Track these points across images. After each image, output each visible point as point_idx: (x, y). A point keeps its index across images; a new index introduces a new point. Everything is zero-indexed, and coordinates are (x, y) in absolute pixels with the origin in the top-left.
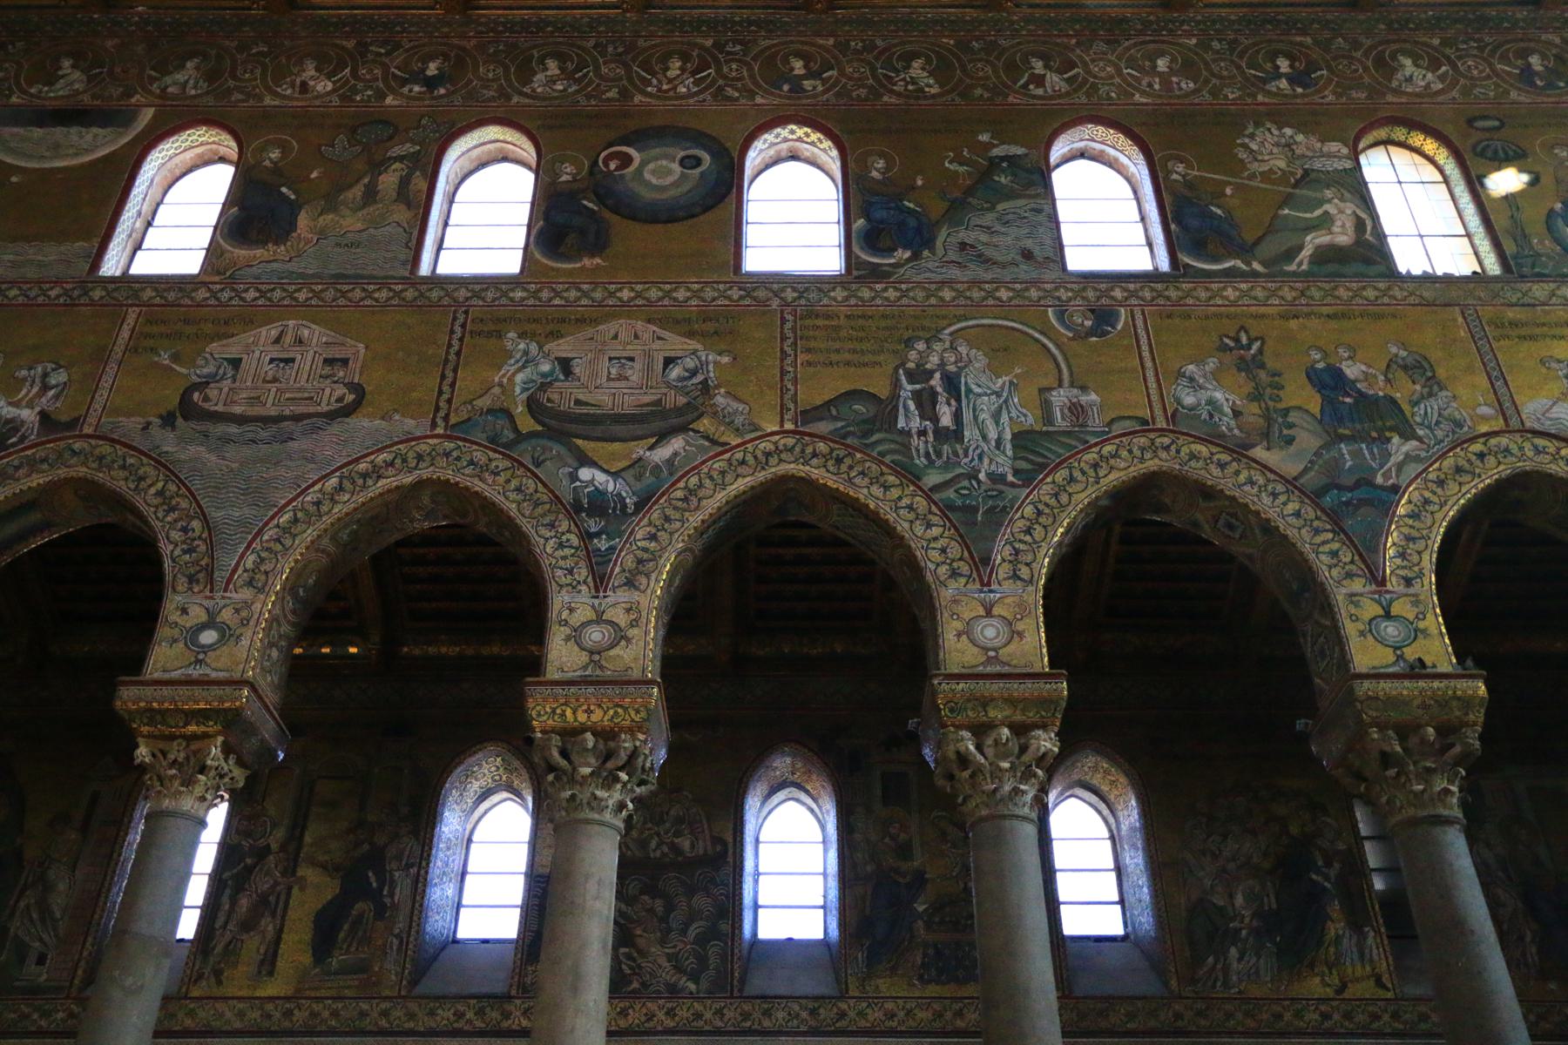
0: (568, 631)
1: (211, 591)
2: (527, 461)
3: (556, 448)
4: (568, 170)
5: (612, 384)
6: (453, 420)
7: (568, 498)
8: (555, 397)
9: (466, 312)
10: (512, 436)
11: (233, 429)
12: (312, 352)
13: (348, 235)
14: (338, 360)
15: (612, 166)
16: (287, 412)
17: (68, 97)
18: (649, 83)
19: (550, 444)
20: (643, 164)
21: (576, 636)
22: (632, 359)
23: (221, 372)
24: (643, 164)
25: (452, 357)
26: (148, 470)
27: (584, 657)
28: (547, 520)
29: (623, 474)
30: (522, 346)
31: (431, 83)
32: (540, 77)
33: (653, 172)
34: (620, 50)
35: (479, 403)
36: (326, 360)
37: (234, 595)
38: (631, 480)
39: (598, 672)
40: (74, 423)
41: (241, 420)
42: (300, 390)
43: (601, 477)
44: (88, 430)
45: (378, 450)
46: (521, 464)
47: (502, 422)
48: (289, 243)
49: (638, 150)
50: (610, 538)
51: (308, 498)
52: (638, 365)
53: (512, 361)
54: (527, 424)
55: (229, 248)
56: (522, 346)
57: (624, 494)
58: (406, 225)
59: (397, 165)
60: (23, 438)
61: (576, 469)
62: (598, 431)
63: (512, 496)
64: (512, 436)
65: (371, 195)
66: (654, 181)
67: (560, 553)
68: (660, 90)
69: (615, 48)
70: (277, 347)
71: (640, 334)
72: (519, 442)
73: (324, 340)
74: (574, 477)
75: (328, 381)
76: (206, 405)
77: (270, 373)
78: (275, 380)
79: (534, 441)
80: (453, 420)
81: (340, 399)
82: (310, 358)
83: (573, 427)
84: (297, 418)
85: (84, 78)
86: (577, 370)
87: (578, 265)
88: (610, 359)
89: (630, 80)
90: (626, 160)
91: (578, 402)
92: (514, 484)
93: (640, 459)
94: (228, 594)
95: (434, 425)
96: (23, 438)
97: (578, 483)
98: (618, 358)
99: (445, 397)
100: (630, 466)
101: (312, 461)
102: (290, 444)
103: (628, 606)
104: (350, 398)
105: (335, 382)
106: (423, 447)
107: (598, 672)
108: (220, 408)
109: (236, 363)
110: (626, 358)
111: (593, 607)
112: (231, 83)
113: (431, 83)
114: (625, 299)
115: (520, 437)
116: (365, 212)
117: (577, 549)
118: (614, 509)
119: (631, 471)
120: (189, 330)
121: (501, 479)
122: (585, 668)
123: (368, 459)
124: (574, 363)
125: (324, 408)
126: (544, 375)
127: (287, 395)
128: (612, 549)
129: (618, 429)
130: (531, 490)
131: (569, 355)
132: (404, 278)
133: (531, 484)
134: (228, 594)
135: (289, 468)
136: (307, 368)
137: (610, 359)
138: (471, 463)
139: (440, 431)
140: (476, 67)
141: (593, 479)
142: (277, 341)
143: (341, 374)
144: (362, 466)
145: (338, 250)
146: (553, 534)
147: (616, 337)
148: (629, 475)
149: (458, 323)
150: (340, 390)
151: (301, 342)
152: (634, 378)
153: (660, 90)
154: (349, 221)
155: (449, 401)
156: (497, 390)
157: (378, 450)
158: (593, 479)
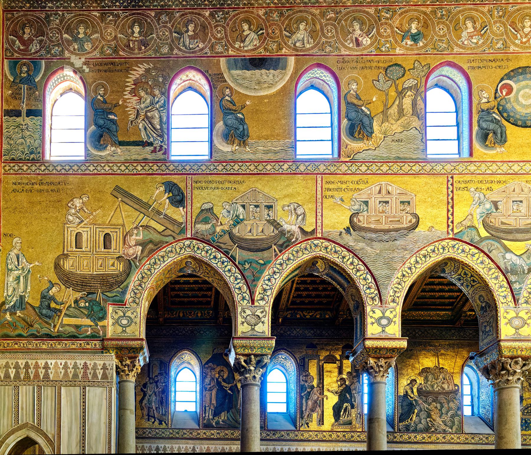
0: (507, 321)
1: (381, 304)
2: (486, 251)
3: (496, 244)
4: (485, 96)
5: (515, 214)
6: (456, 231)
7: (502, 267)
8: (493, 220)
9: (452, 178)
10: (478, 238)
11: (374, 236)
12: (394, 198)
13: (396, 135)
14: (406, 202)
15: (504, 93)
16: (391, 227)
17: (253, 50)
18: (516, 38)
19: (493, 242)
20: (519, 91)
21: (510, 322)
22: (521, 202)
23: (362, 207)
24: (519, 91)
25: (450, 201)
26: (346, 253)
27: (513, 331)
28: (494, 276)
29: (522, 256)
30: (477, 195)
31: (415, 38)
32: (464, 34)
33: (523, 96)
34: (501, 13)
35: (464, 223)
36: (401, 202)
37: (389, 306)
38: (526, 259)
39: (519, 336)
40: (313, 232)
41: (375, 231)
42: (394, 217)
43: (514, 258)
44: (319, 235)
45: (429, 245)
46: (483, 252)
47: (474, 232)
48: (373, 140)
49: (515, 82)
50: (520, 284)
51: (406, 266)
52: (525, 204)
53: (474, 203)
54: (484, 233)
55: (349, 143)
56: (477, 195)
57: (523, 265)
58: (419, 129)
59: (409, 93)
60: (297, 239)
61: (505, 254)
62: (510, 237)
63: (481, 266)
64: (478, 238)
65: (401, 112)
66: (524, 102)
67: (500, 290)
68: (522, 42)
69: (498, 13)
70: (380, 196)
71: (524, 189)
72: (481, 242)
73: (398, 192)
74: (504, 258)
75: (404, 212)
76: (360, 224)
77: (381, 208)
78: (383, 212)
79: (487, 242)
80: (456, 231)
81: (410, 221)
82: (394, 201)
83: (502, 235)
84: (397, 230)
85: (256, 37)
86: (500, 207)
87: (495, 152)
88: (513, 201)
89: (507, 34)
90: (510, 90)
91: (502, 223)
92: (481, 259)
93: (528, 249)
94: (387, 305)
95: (448, 233)
96: (297, 239)
97: (506, 260)
98: (516, 201)
99: (450, 220)
100: (525, 253)
101: (406, 250)
102: (396, 242)
103: (527, 311)
104: (414, 220)
105: (407, 213)
106: (444, 243)
107: (519, 336)
108: (365, 225)
109: (366, 203)
110: (519, 201)
111: (515, 311)
112: (324, 40)
113: (415, 38)
114: (516, 171)
115: (482, 239)
116: (400, 122)
117: (507, 288)
118: (520, 271)
119: (525, 255)
120: (344, 186)
121: (475, 259)
122: (514, 334)
123: (425, 249)
124: (499, 203)
125: (405, 226)
126: (487, 210)
127: (390, 219)
128: (521, 288)
129: (519, 236)
130: (487, 263)
131: (497, 200)
132: (424, 159)
133: (487, 260)
134: (387, 305)
135: (398, 253)
136: (395, 206)
137: (513, 201)
138: (463, 251)
139: (451, 236)
140: (434, 29)
141: (511, 259)
142: (380, 192)
143: (408, 209)
144: (423, 252)
145: (394, 143)
146: (497, 282)
147: (514, 191)
148: (524, 256)
149: (450, 183)
150: (410, 217)
151: (389, 193)
152: (523, 211)
153: (522, 42)
154: (394, 127)
155: (452, 222)
156: (470, 217)
157: (429, 245)
158: (511, 259)
